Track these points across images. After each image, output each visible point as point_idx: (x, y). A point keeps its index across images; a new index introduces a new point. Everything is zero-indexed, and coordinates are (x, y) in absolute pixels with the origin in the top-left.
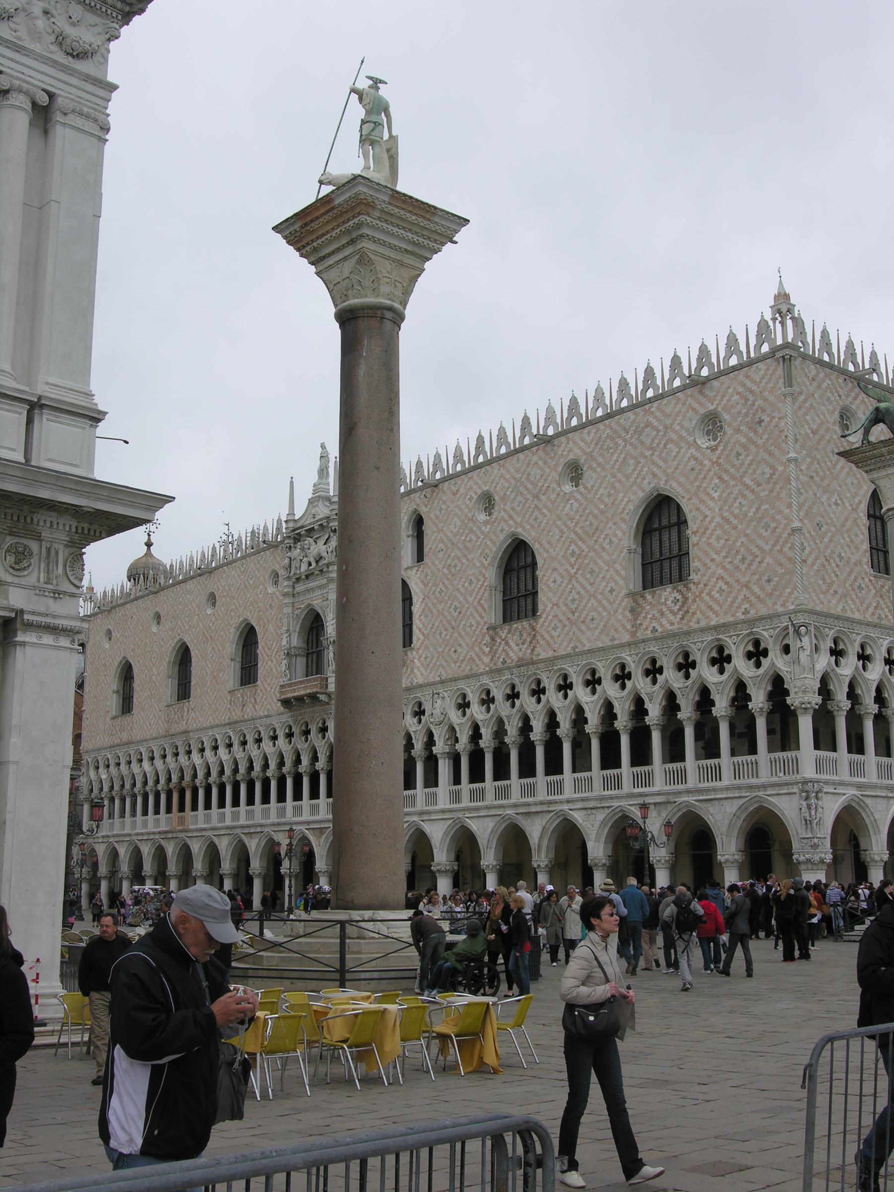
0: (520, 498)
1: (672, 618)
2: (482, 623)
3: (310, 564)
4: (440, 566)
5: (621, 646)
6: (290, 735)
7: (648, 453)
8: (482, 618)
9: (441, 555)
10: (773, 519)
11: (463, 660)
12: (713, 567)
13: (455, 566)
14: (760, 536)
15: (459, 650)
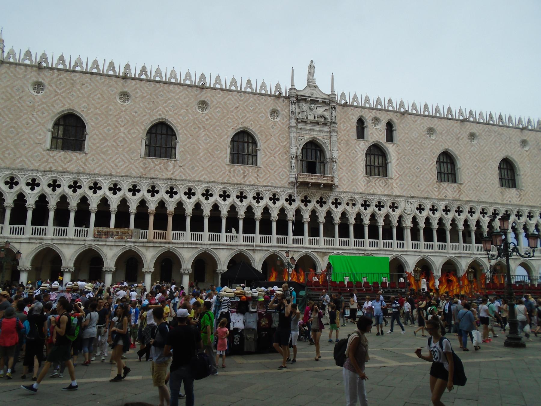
2: (433, 179)
3: (315, 118)
4: (408, 148)
5: (498, 204)
6: (290, 200)
7: (504, 143)
9: (407, 144)
11: (423, 191)
13: (416, 151)
15: (421, 186)
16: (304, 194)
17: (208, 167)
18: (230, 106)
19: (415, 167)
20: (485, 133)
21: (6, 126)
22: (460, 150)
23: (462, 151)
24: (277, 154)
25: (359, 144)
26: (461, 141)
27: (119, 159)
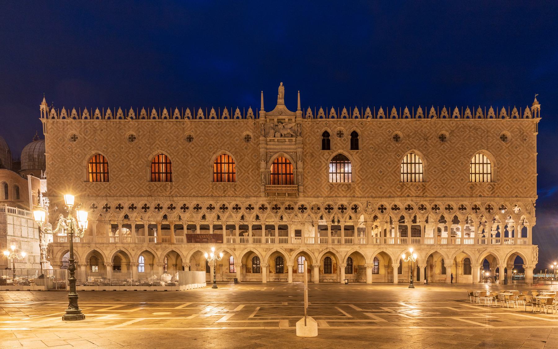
0: (417, 138)
1: (488, 193)
2: (396, 180)
7: (480, 138)
8: (396, 178)
9: (372, 150)
10: (528, 170)
12: (505, 180)
13: (380, 156)
14: (523, 174)
15: (383, 188)
16: (275, 203)
17: (196, 186)
18: (210, 134)
19: (378, 170)
20: (459, 130)
21: (58, 167)
22: (428, 150)
23: (429, 150)
24: (250, 171)
25: (324, 154)
26: (430, 141)
27: (132, 185)
